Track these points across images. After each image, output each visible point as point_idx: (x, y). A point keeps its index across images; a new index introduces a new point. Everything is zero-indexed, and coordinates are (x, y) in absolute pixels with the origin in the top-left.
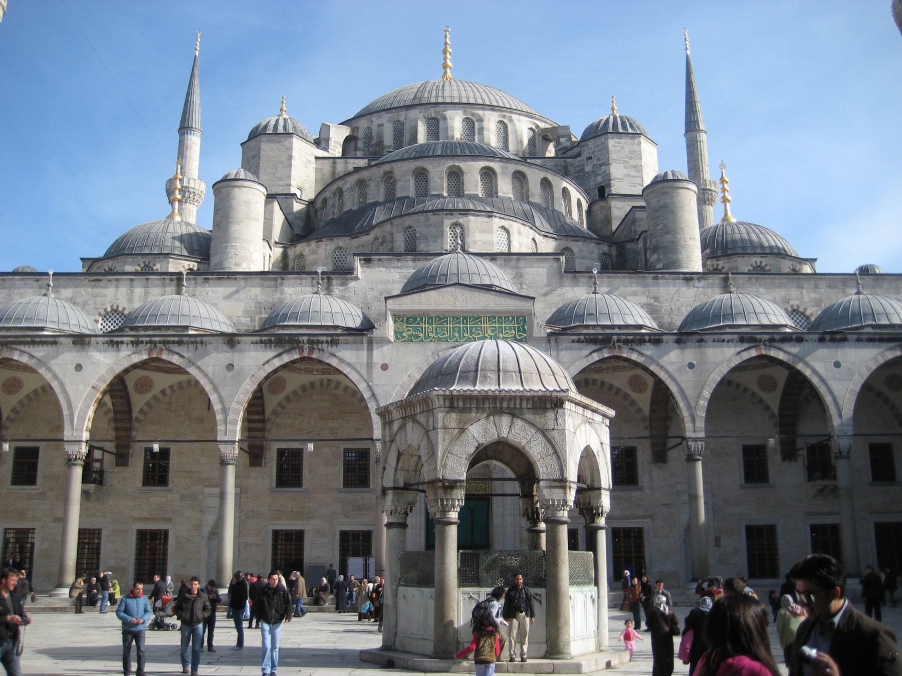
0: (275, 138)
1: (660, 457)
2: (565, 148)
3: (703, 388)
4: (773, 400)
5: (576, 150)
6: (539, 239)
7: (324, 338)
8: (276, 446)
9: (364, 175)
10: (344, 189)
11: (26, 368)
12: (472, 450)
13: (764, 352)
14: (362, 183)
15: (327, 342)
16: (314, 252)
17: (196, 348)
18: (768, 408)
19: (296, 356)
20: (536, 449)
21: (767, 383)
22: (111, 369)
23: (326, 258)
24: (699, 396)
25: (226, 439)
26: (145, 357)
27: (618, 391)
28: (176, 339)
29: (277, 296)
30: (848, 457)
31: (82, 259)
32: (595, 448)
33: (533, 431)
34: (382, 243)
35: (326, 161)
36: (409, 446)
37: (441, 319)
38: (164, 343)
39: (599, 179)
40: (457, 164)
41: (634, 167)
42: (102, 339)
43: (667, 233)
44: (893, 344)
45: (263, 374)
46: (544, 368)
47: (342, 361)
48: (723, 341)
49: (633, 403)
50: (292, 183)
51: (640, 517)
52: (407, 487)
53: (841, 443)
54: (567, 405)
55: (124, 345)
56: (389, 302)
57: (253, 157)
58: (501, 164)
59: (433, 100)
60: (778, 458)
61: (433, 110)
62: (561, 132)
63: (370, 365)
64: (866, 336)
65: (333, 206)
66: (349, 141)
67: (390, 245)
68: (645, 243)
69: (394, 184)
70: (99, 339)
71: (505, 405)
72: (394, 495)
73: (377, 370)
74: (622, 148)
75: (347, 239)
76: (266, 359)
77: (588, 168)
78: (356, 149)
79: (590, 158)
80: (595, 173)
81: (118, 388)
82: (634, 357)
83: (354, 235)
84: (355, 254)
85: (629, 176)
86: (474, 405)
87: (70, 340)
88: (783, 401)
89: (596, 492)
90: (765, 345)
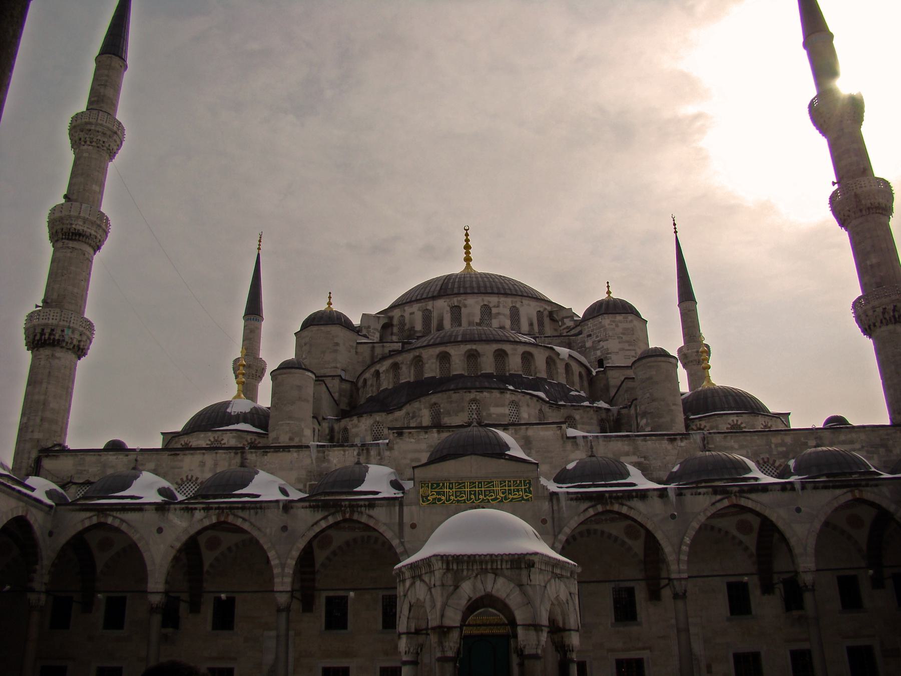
0: (323, 328)
1: (654, 595)
2: (568, 327)
3: (684, 535)
4: (750, 541)
6: (546, 408)
7: (362, 503)
8: (324, 594)
9: (399, 359)
10: (381, 371)
11: (117, 530)
12: (464, 602)
13: (735, 502)
14: (396, 367)
15: (365, 506)
16: (356, 426)
17: (256, 513)
18: (746, 549)
19: (339, 518)
20: (514, 600)
23: (366, 430)
24: (682, 542)
25: (281, 588)
27: (616, 538)
28: (240, 505)
29: (325, 465)
30: (813, 590)
31: (162, 433)
32: (563, 596)
33: (512, 585)
34: (413, 417)
35: (366, 346)
36: (418, 599)
37: (460, 484)
38: (231, 508)
39: (599, 353)
40: (474, 347)
41: (627, 342)
42: (179, 506)
43: (653, 400)
44: (845, 490)
45: (312, 534)
47: (377, 521)
48: (700, 494)
50: (338, 365)
51: (639, 649)
52: (418, 632)
53: (807, 578)
54: (537, 565)
55: (198, 511)
56: (416, 470)
57: (305, 344)
58: (512, 346)
59: (456, 291)
60: (758, 592)
61: (455, 299)
62: (564, 314)
63: (401, 524)
64: (821, 485)
65: (372, 385)
66: (387, 327)
67: (419, 420)
68: (636, 410)
69: (422, 366)
70: (177, 506)
71: (489, 567)
72: (407, 639)
73: (407, 529)
74: (617, 326)
75: (384, 414)
76: (315, 521)
77: (589, 344)
78: (392, 334)
79: (590, 336)
80: (594, 348)
82: (624, 510)
83: (390, 412)
84: (389, 429)
85: (623, 349)
86: (465, 567)
87: (154, 507)
89: (567, 633)
90: (736, 496)
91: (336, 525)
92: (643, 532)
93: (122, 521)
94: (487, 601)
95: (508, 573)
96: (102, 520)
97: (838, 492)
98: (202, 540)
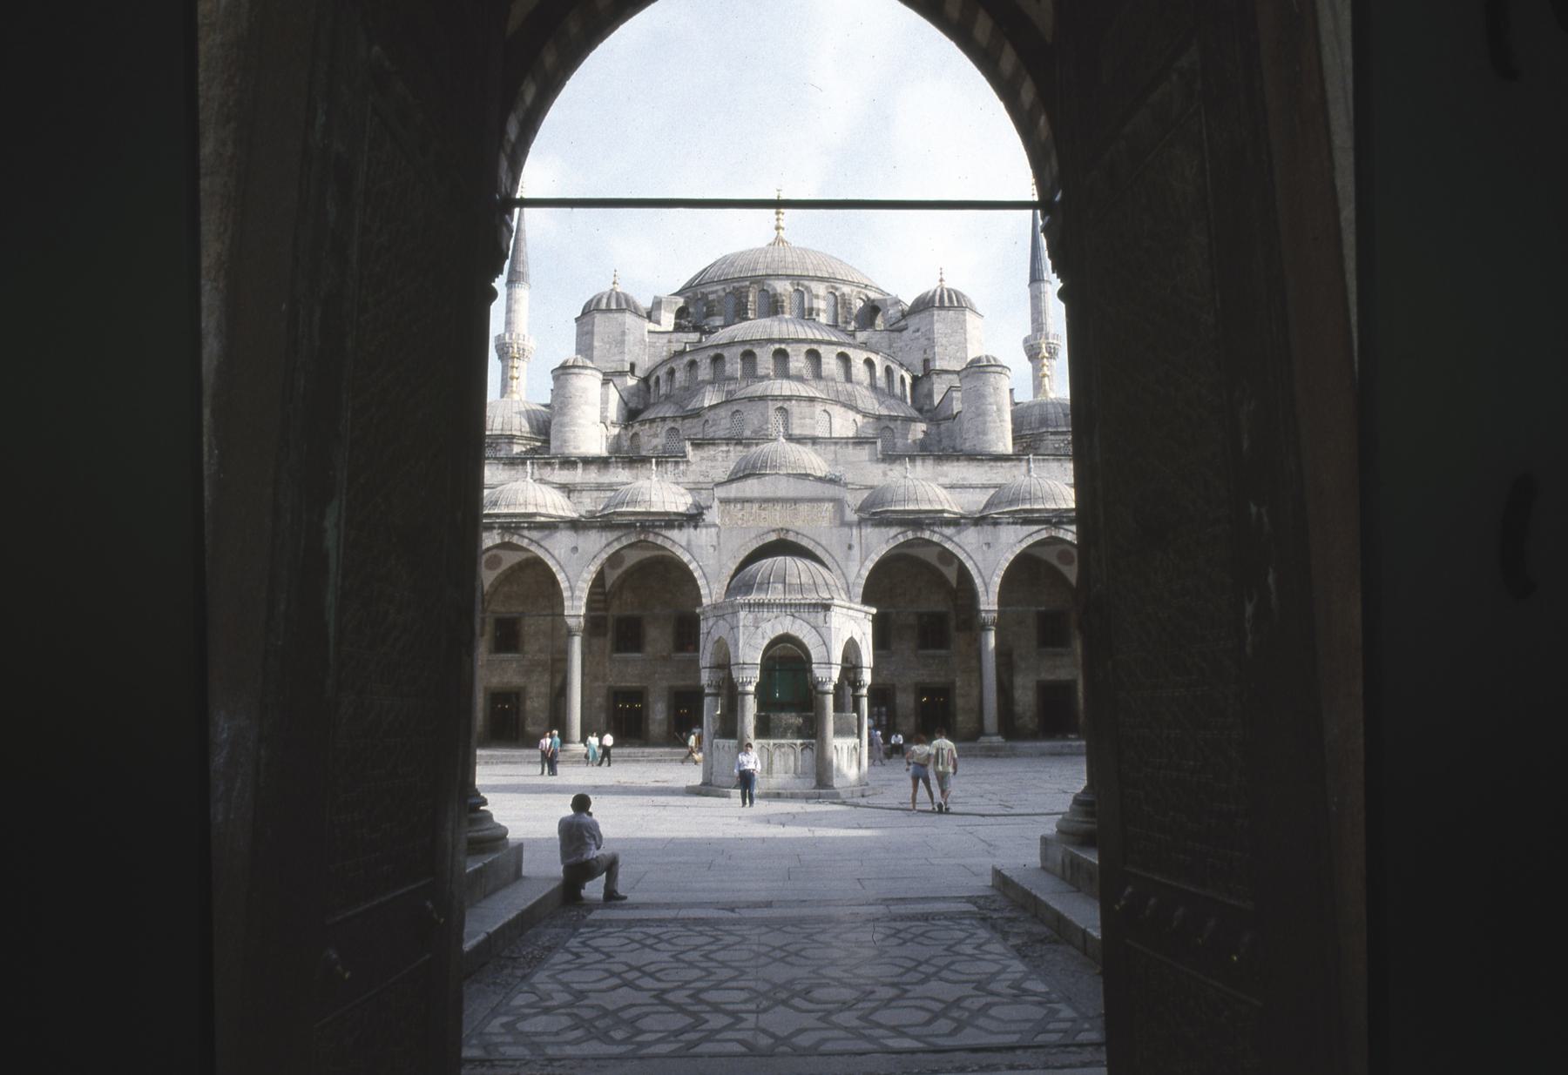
12: (766, 642)
14: (693, 364)
19: (634, 539)
26: (498, 541)
45: (605, 556)
46: (819, 581)
49: (941, 575)
82: (936, 538)
91: (631, 546)
94: (785, 639)
95: (805, 615)
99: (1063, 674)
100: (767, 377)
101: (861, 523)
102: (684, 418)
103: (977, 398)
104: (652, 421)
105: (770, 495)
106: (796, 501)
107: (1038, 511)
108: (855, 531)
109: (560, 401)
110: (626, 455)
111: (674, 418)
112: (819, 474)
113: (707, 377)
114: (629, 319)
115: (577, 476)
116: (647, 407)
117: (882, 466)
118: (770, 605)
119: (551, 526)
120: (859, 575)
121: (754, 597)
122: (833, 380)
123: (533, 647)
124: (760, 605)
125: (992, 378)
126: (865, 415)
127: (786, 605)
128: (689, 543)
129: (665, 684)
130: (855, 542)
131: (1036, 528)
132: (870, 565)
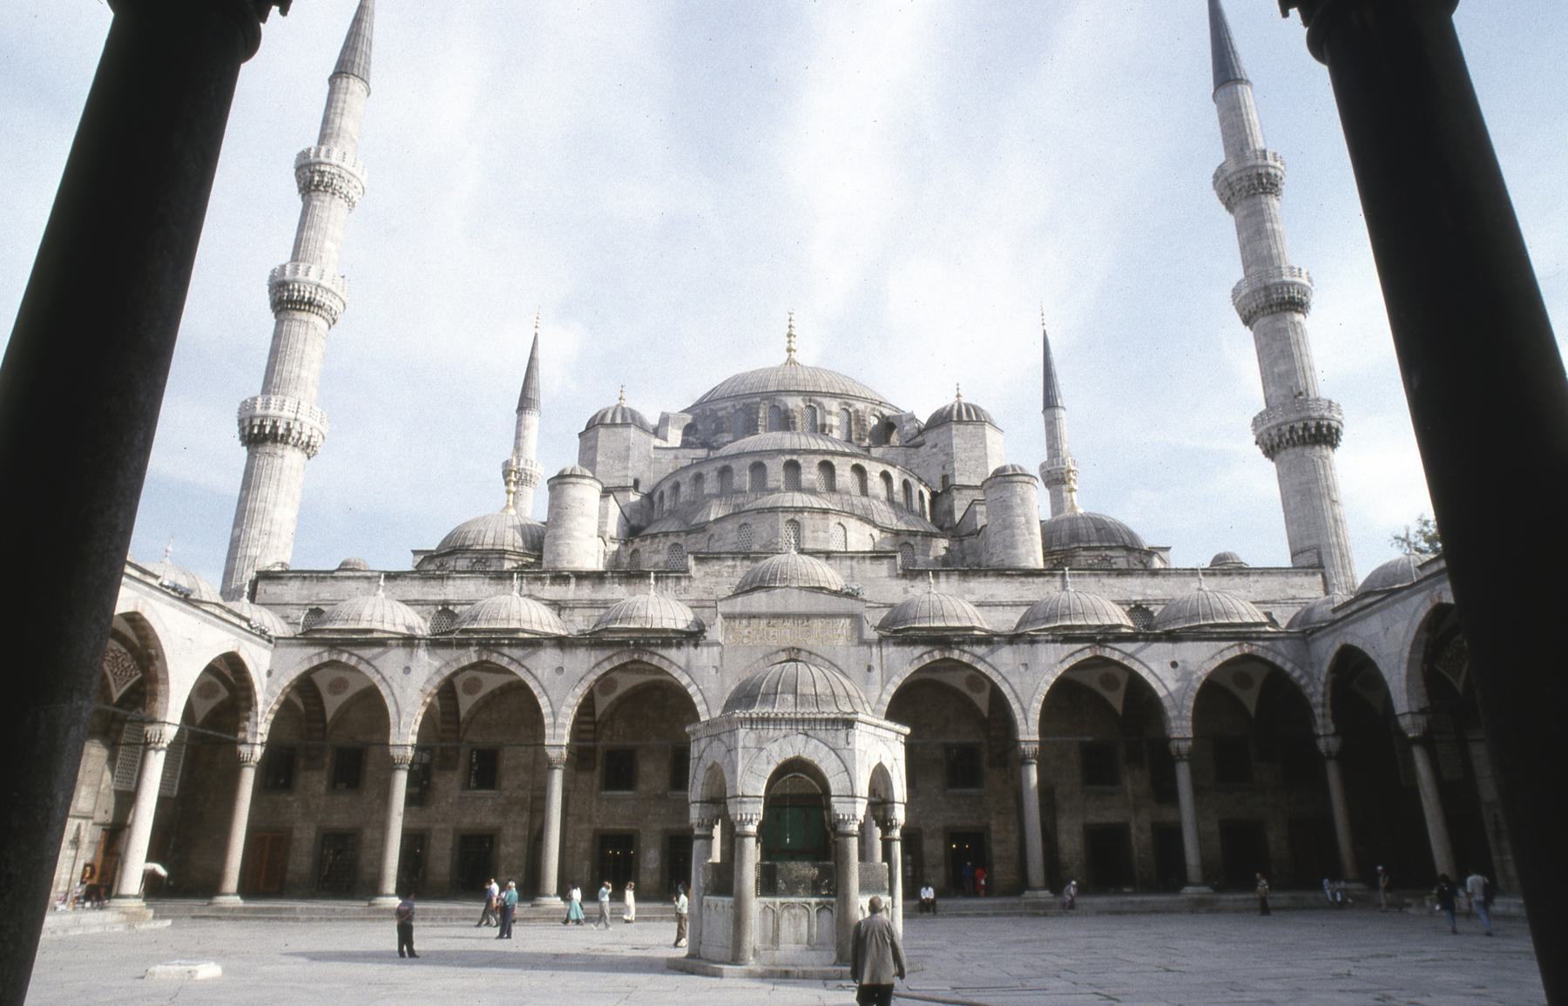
4: (1116, 700)
5: (919, 439)
11: (353, 669)
12: (772, 768)
14: (699, 478)
19: (625, 659)
21: (1110, 682)
22: (438, 671)
25: (553, 742)
26: (475, 659)
31: (415, 552)
45: (593, 677)
46: (839, 691)
49: (971, 705)
81: (447, 691)
82: (966, 659)
88: (1125, 700)
91: (622, 668)
92: (988, 686)
93: (360, 658)
95: (822, 734)
96: (335, 657)
97: (1224, 644)
98: (459, 683)
99: (1112, 816)
100: (777, 490)
101: (881, 642)
102: (688, 533)
103: (1003, 510)
104: (654, 536)
105: (779, 609)
106: (808, 617)
107: (1080, 627)
108: (874, 650)
109: (558, 509)
110: (626, 571)
111: (677, 533)
112: (834, 588)
113: (714, 491)
114: (633, 433)
115: (569, 592)
116: (650, 523)
117: (904, 583)
118: (776, 721)
119: (535, 643)
120: (879, 701)
121: (757, 711)
122: (848, 493)
123: (512, 782)
124: (765, 720)
125: (1019, 488)
126: (883, 529)
127: (797, 721)
128: (688, 664)
129: (658, 827)
130: (875, 663)
131: (1079, 646)
132: (892, 689)
